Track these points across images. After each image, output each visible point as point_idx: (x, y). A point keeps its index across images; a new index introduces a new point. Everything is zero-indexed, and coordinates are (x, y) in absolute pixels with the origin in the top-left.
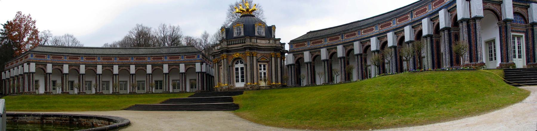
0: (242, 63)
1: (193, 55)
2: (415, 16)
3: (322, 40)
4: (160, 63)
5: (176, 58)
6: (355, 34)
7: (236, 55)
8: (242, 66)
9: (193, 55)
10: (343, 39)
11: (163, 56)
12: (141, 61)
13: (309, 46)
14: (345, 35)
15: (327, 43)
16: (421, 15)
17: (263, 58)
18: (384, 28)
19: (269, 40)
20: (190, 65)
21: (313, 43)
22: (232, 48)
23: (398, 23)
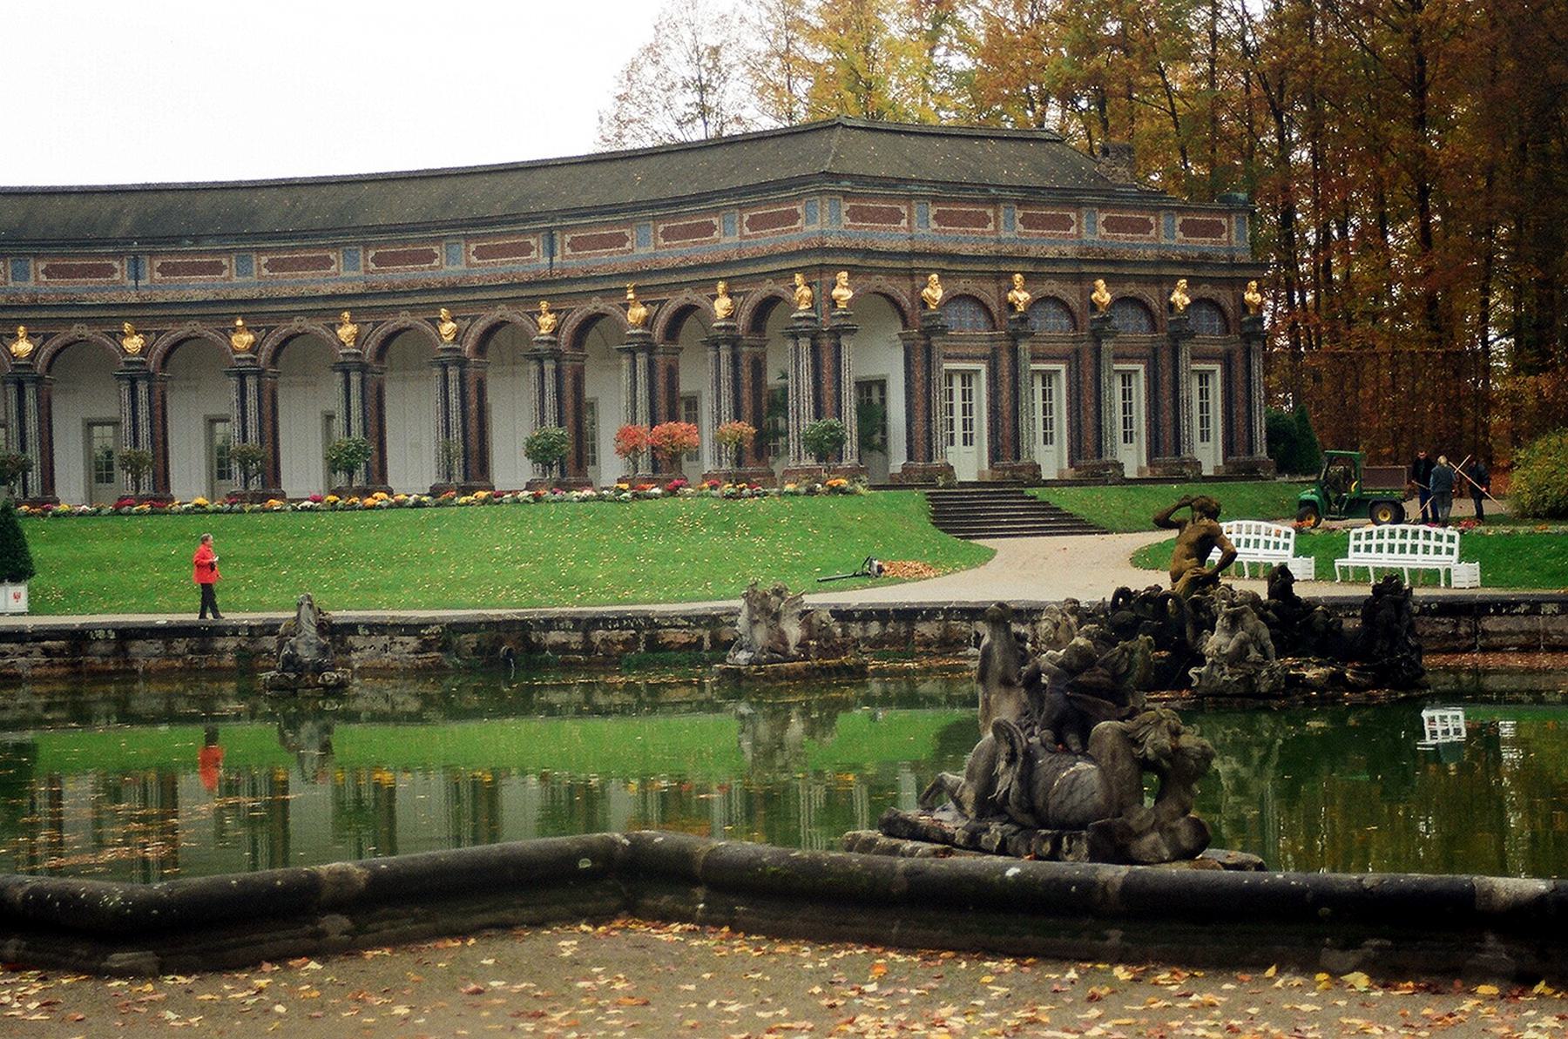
2: (568, 251)
6: (216, 268)
10: (137, 278)
14: (151, 263)
15: (31, 284)
16: (597, 254)
18: (398, 270)
23: (474, 259)
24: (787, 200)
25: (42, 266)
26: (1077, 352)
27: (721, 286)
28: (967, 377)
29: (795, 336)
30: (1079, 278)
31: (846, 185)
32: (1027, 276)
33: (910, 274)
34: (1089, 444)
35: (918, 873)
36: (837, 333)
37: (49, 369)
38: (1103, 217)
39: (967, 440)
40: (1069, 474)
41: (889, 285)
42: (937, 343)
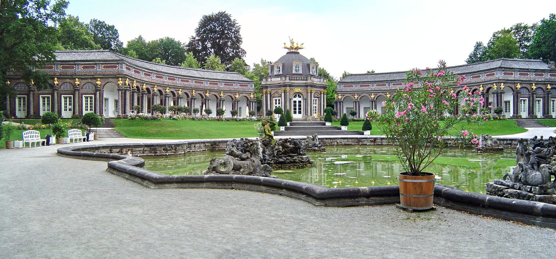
0: (300, 97)
1: (246, 84)
3: (370, 85)
4: (216, 89)
5: (230, 85)
6: (401, 84)
7: (297, 90)
8: (300, 99)
9: (246, 84)
11: (219, 82)
12: (199, 84)
13: (357, 88)
15: (374, 87)
17: (316, 94)
19: (320, 79)
20: (243, 93)
21: (360, 86)
22: (295, 83)
24: (493, 72)
25: (376, 84)
26: (544, 96)
27: (481, 86)
28: (524, 101)
29: (494, 94)
30: (545, 84)
31: (503, 69)
32: (535, 84)
33: (514, 83)
34: (546, 112)
35: (491, 200)
36: (501, 93)
37: (376, 100)
38: (549, 74)
39: (524, 111)
40: (543, 117)
41: (510, 85)
42: (519, 95)
